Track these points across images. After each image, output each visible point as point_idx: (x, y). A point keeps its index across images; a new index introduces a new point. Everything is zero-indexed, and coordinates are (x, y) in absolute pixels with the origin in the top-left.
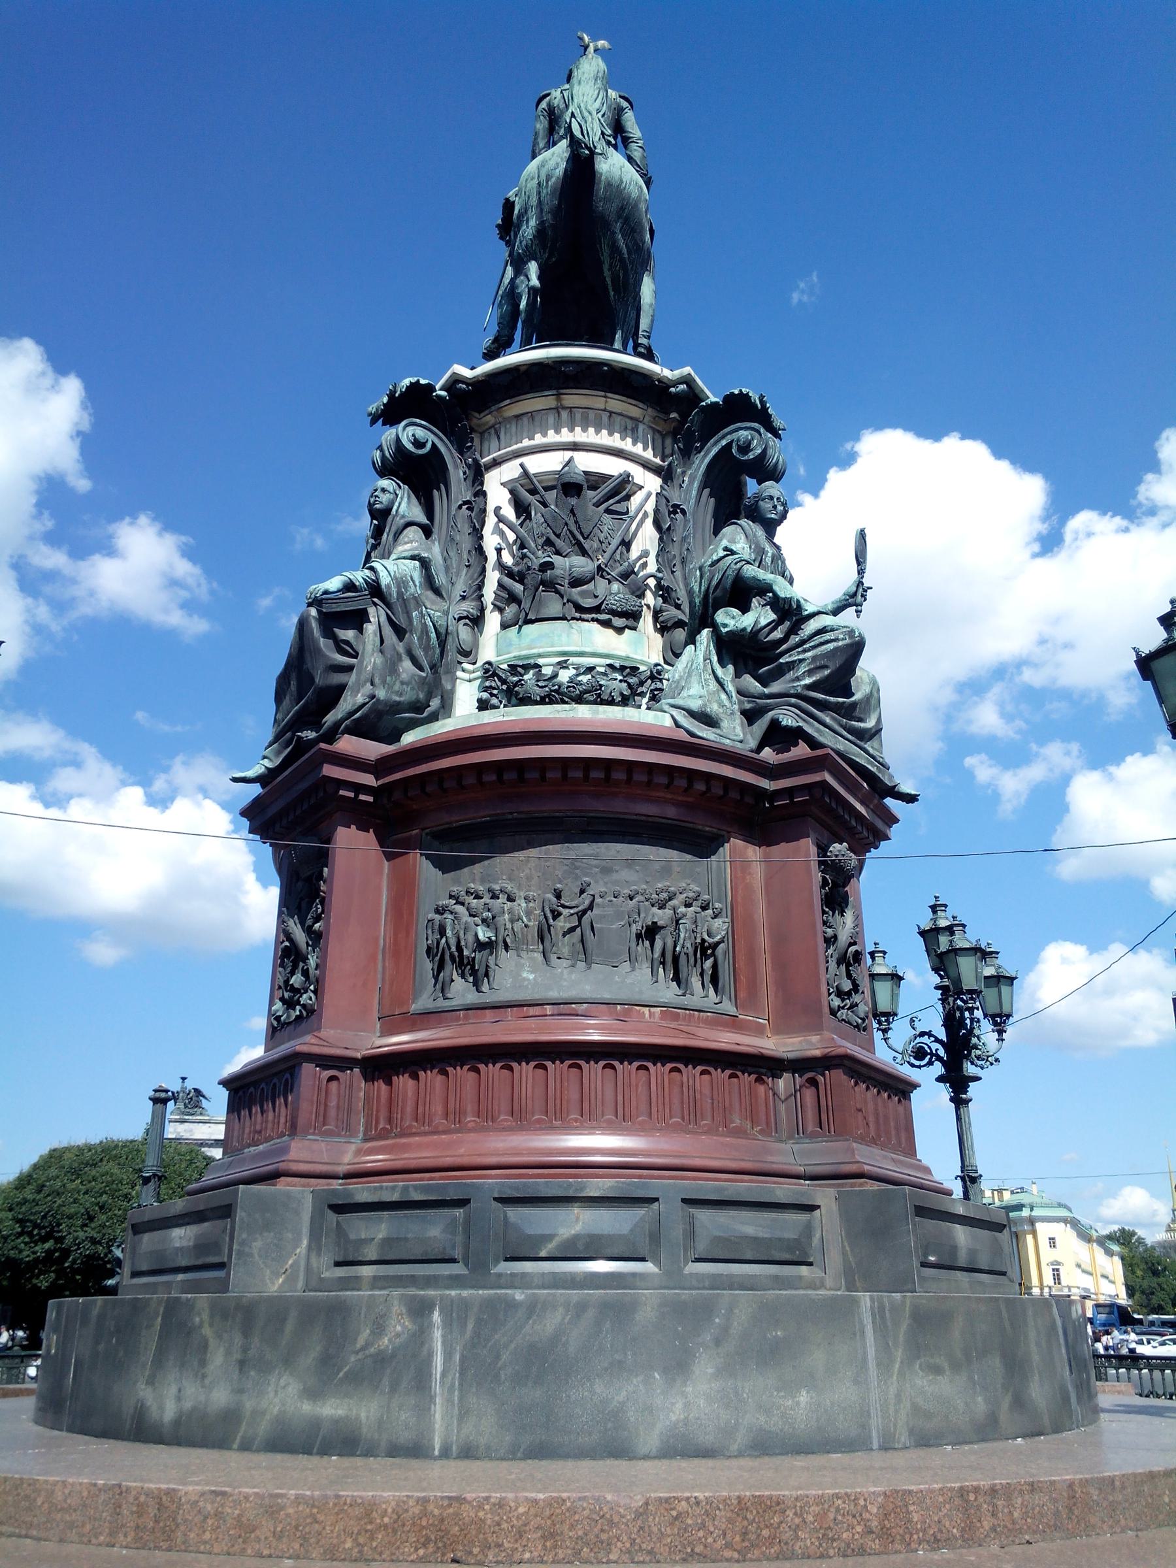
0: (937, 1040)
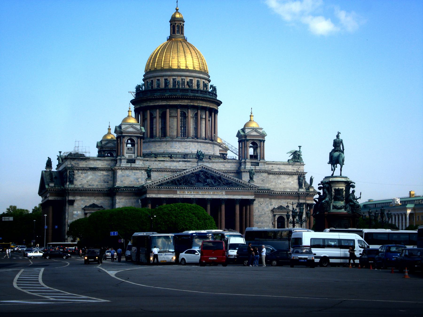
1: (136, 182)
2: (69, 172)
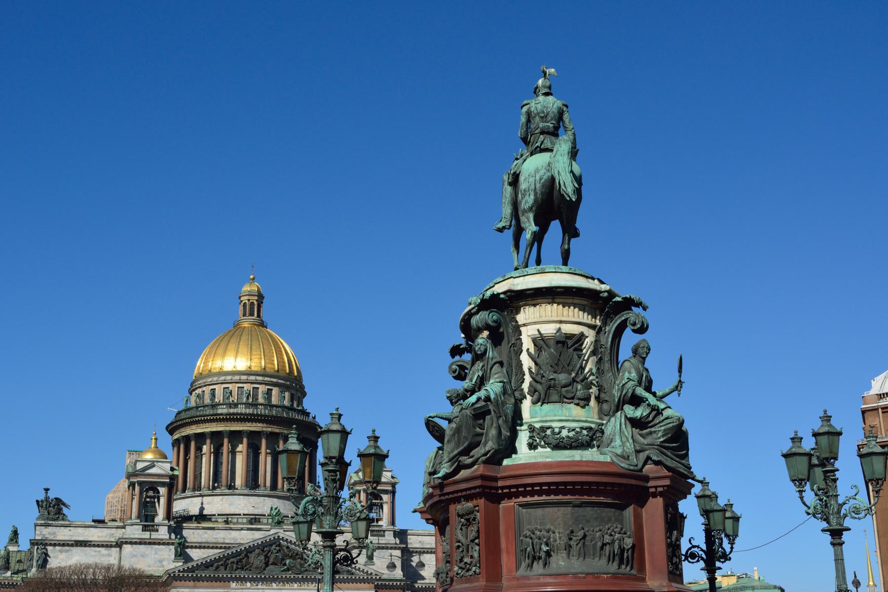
0: (702, 550)
1: (158, 567)
2: (38, 548)
